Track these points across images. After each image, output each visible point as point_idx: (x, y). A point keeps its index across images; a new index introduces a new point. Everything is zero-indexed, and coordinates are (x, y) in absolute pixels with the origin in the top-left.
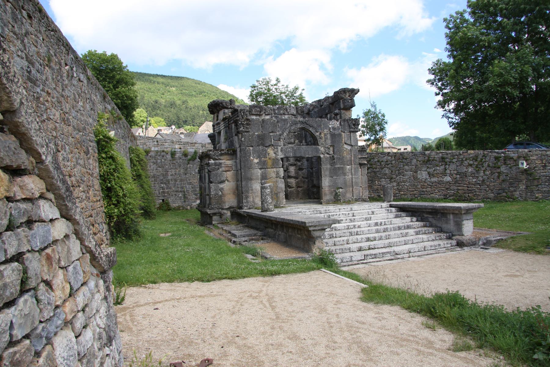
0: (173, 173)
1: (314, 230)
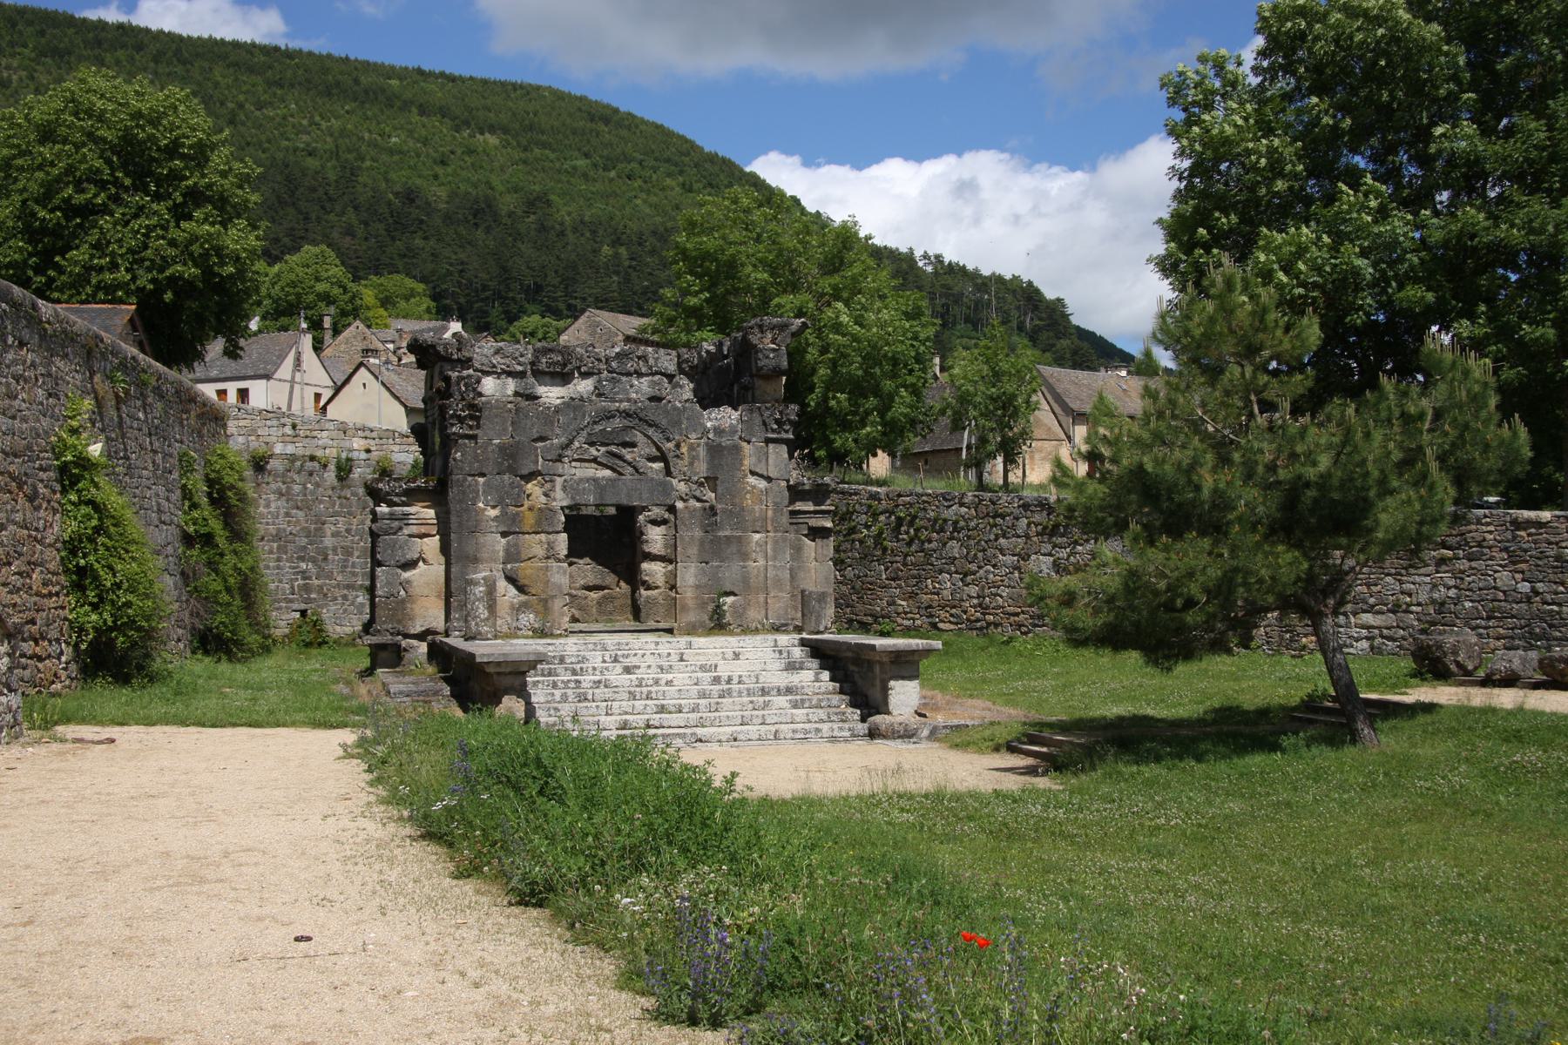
0: (342, 527)
1: (499, 674)
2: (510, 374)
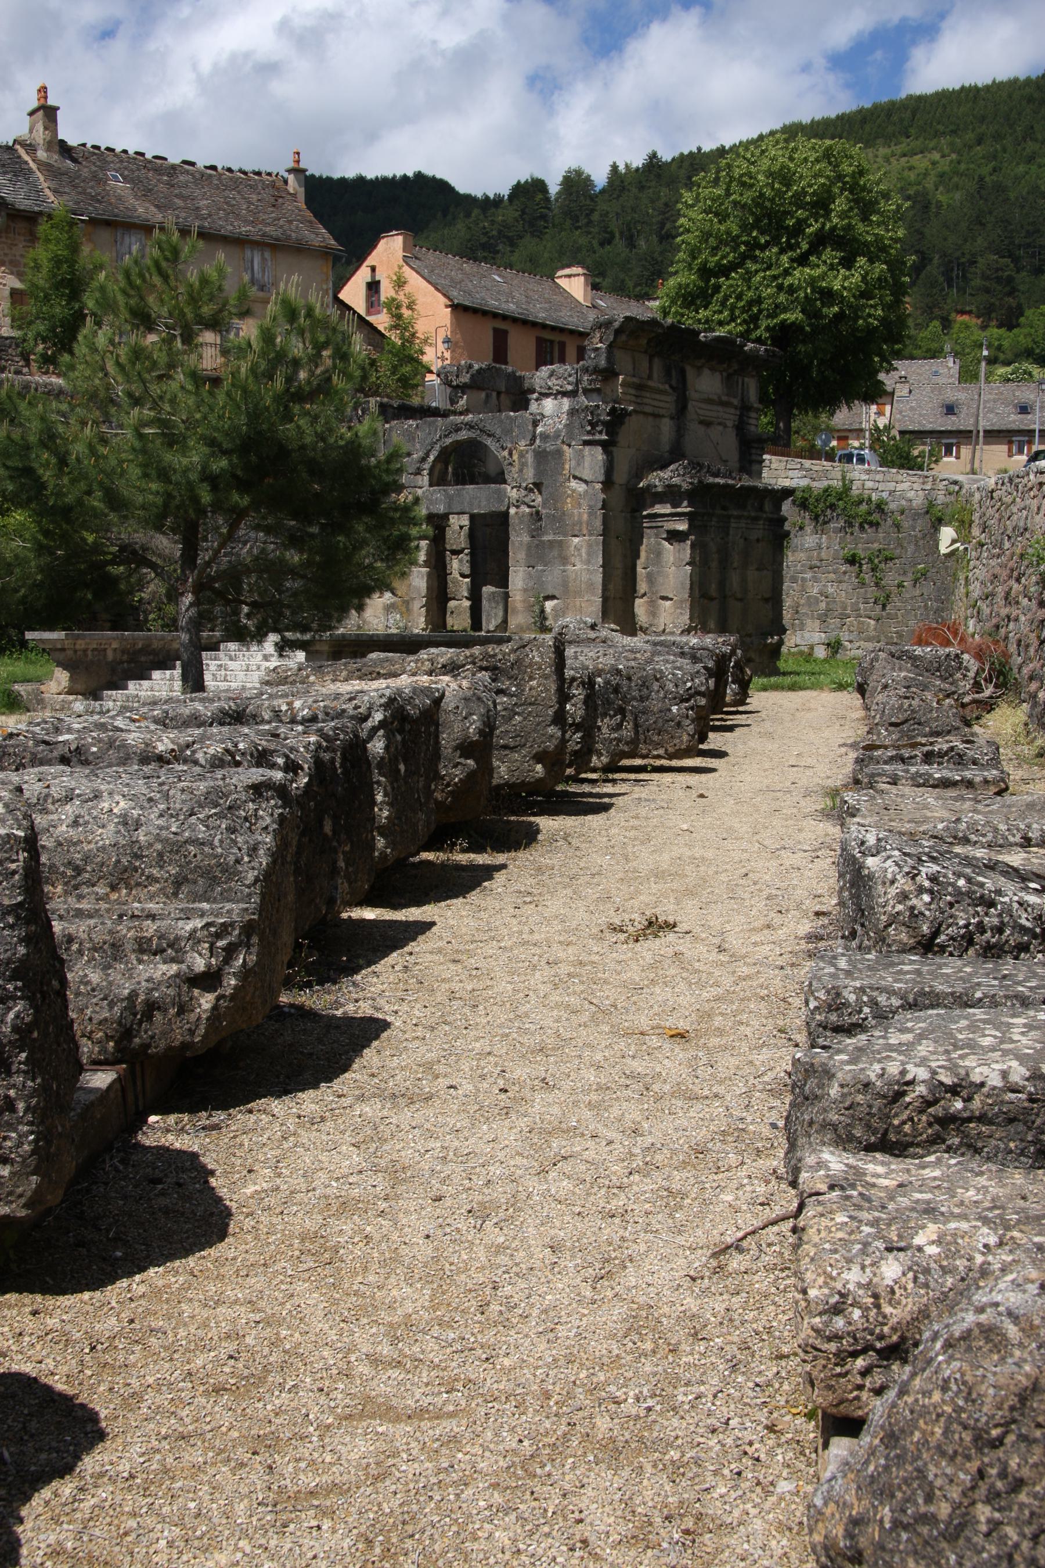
2: (565, 394)
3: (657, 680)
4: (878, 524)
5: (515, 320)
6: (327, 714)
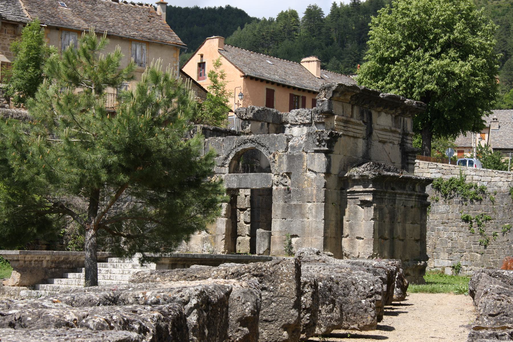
2: (304, 125)
3: (353, 284)
4: (481, 200)
5: (278, 85)
6: (165, 300)
